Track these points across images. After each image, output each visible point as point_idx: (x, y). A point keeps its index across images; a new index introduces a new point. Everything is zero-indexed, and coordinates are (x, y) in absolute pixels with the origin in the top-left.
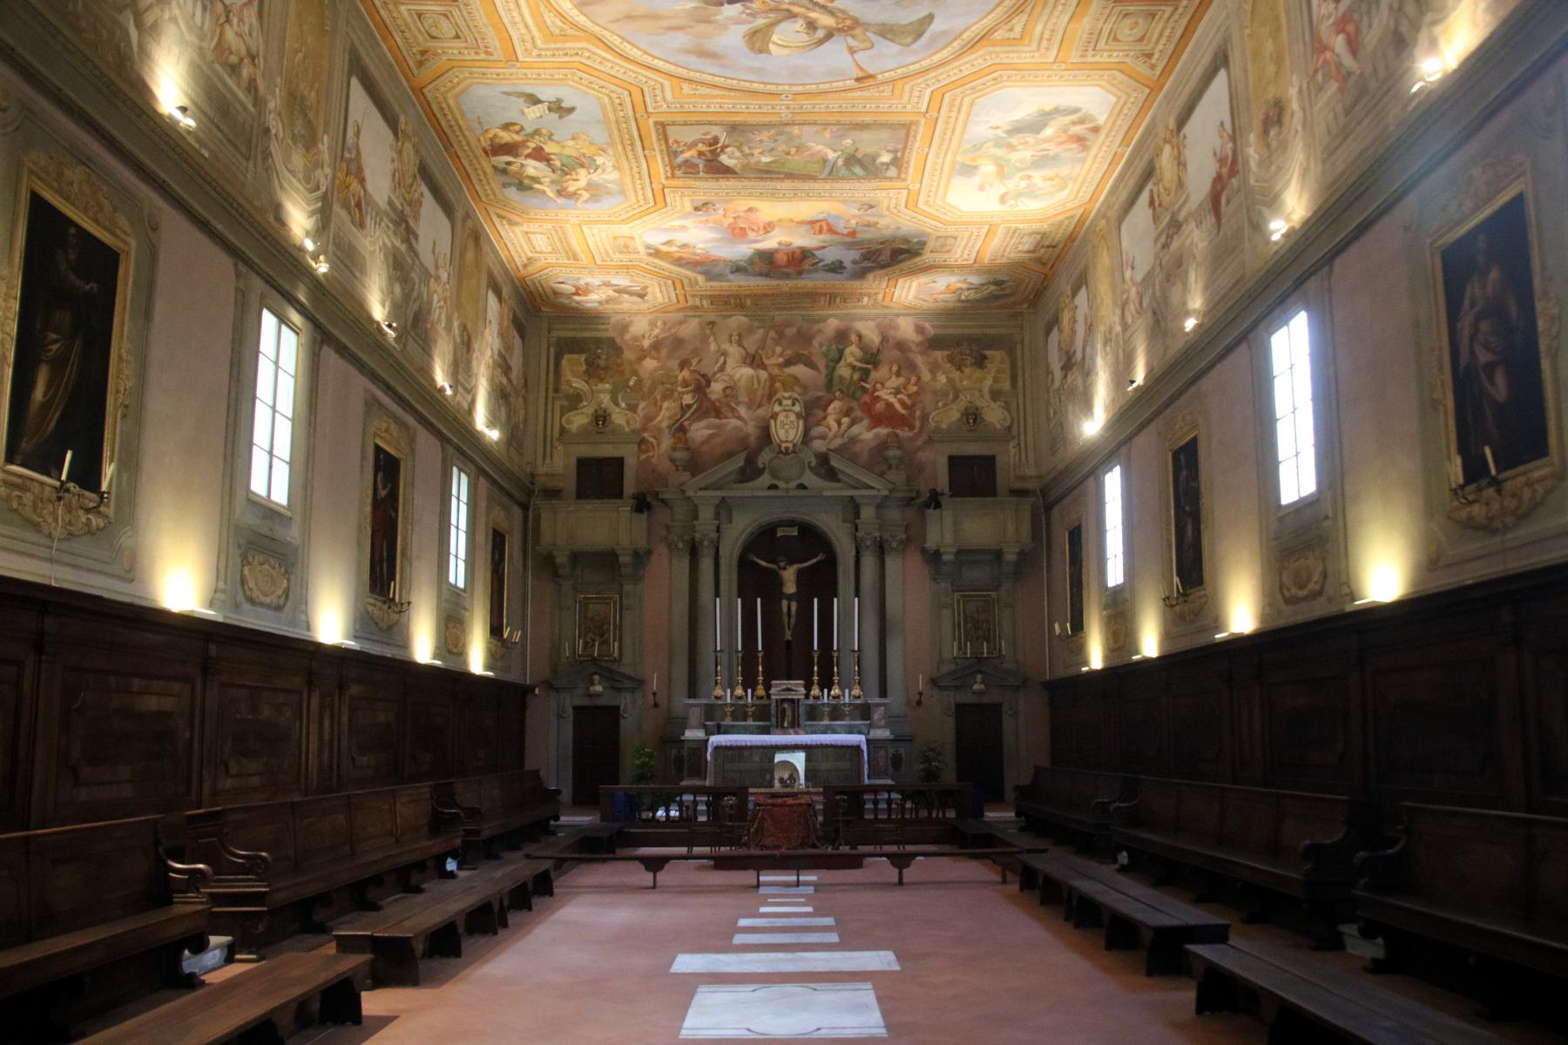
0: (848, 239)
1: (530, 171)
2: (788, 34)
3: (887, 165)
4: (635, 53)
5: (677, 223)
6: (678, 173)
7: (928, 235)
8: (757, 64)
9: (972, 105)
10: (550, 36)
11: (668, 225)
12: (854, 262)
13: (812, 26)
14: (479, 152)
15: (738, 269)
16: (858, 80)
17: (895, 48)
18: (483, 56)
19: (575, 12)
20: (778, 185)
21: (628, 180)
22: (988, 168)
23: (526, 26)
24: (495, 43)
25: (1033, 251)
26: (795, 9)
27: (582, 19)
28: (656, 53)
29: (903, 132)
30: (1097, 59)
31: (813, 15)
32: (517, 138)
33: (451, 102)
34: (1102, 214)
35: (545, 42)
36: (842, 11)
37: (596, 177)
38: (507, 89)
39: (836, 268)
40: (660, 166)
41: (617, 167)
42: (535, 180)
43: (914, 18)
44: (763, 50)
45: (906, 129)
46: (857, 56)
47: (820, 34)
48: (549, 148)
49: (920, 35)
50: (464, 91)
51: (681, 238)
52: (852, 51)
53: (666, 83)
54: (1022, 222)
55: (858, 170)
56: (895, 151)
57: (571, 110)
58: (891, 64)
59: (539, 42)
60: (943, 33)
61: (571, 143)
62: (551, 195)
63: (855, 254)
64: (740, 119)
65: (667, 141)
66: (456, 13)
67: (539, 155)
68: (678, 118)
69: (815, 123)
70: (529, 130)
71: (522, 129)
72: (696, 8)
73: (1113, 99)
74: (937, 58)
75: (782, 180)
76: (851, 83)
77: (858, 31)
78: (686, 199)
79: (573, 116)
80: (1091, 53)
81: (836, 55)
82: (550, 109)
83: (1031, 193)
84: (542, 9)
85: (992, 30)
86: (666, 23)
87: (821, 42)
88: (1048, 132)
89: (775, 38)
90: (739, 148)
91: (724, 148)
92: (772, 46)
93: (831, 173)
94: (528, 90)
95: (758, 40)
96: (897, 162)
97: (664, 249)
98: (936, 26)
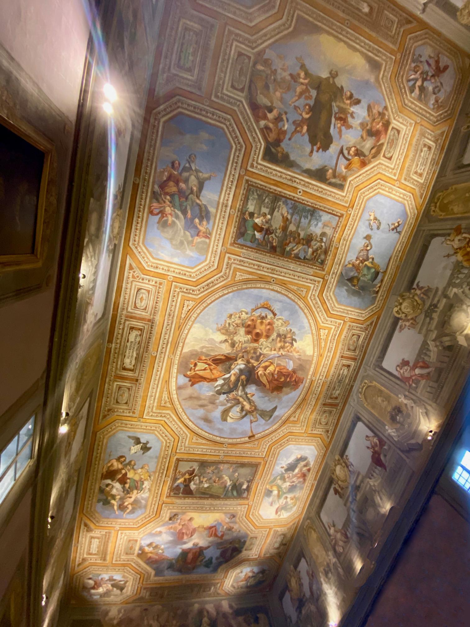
0: (219, 541)
1: (114, 492)
2: (235, 412)
3: (245, 490)
4: (185, 417)
5: (158, 529)
6: (172, 494)
7: (246, 536)
8: (220, 427)
9: (278, 454)
10: (160, 407)
11: (154, 532)
12: (217, 558)
13: (242, 409)
14: (99, 476)
15: (171, 566)
16: (250, 437)
17: (264, 421)
18: (131, 414)
19: (175, 392)
20: (206, 502)
21: (152, 497)
22: (275, 492)
23: (154, 399)
24: (138, 408)
25: (278, 548)
26: (241, 400)
27: (175, 396)
28: (191, 419)
29: (255, 469)
30: (315, 432)
31: (245, 403)
32: (120, 466)
33: (105, 441)
34: (307, 517)
35: (157, 409)
36: (253, 402)
37: (139, 496)
38: (131, 435)
39: (208, 564)
40: (166, 490)
41: (150, 490)
42: (114, 497)
43: (271, 408)
44: (224, 419)
45: (255, 466)
46: (253, 424)
47: (244, 413)
48: (130, 475)
49: (271, 417)
50: (114, 433)
51: (157, 540)
52: (251, 422)
53: (189, 435)
54: (279, 526)
55: (235, 493)
56: (248, 482)
57: (150, 448)
58: (261, 429)
59: (154, 409)
60: (277, 416)
61: (140, 470)
62: (116, 507)
63: (218, 553)
64: (206, 458)
65: (176, 470)
66: (134, 388)
67: (123, 481)
68: (185, 457)
69: (227, 463)
70: (127, 461)
71: (125, 460)
72: (213, 395)
73: (317, 453)
74: (274, 427)
75: (207, 498)
76: (247, 439)
77: (254, 413)
78: (169, 511)
79: (151, 450)
80: (314, 429)
81: (246, 425)
82: (141, 448)
83: (284, 508)
84: (165, 389)
85: (289, 417)
86: (201, 402)
87: (243, 417)
88: (297, 471)
89: (230, 414)
90: (199, 477)
91: (195, 476)
92: (228, 418)
93: (225, 495)
94: (139, 435)
95: (225, 414)
96: (248, 489)
97: (147, 549)
98: (276, 413)
